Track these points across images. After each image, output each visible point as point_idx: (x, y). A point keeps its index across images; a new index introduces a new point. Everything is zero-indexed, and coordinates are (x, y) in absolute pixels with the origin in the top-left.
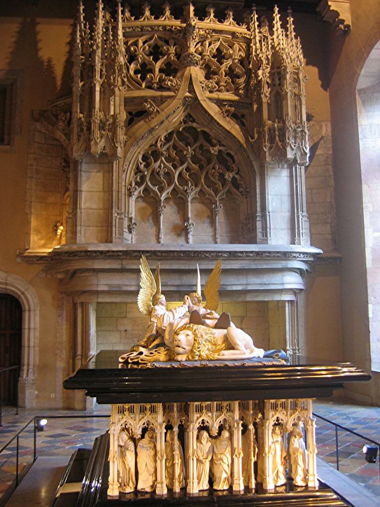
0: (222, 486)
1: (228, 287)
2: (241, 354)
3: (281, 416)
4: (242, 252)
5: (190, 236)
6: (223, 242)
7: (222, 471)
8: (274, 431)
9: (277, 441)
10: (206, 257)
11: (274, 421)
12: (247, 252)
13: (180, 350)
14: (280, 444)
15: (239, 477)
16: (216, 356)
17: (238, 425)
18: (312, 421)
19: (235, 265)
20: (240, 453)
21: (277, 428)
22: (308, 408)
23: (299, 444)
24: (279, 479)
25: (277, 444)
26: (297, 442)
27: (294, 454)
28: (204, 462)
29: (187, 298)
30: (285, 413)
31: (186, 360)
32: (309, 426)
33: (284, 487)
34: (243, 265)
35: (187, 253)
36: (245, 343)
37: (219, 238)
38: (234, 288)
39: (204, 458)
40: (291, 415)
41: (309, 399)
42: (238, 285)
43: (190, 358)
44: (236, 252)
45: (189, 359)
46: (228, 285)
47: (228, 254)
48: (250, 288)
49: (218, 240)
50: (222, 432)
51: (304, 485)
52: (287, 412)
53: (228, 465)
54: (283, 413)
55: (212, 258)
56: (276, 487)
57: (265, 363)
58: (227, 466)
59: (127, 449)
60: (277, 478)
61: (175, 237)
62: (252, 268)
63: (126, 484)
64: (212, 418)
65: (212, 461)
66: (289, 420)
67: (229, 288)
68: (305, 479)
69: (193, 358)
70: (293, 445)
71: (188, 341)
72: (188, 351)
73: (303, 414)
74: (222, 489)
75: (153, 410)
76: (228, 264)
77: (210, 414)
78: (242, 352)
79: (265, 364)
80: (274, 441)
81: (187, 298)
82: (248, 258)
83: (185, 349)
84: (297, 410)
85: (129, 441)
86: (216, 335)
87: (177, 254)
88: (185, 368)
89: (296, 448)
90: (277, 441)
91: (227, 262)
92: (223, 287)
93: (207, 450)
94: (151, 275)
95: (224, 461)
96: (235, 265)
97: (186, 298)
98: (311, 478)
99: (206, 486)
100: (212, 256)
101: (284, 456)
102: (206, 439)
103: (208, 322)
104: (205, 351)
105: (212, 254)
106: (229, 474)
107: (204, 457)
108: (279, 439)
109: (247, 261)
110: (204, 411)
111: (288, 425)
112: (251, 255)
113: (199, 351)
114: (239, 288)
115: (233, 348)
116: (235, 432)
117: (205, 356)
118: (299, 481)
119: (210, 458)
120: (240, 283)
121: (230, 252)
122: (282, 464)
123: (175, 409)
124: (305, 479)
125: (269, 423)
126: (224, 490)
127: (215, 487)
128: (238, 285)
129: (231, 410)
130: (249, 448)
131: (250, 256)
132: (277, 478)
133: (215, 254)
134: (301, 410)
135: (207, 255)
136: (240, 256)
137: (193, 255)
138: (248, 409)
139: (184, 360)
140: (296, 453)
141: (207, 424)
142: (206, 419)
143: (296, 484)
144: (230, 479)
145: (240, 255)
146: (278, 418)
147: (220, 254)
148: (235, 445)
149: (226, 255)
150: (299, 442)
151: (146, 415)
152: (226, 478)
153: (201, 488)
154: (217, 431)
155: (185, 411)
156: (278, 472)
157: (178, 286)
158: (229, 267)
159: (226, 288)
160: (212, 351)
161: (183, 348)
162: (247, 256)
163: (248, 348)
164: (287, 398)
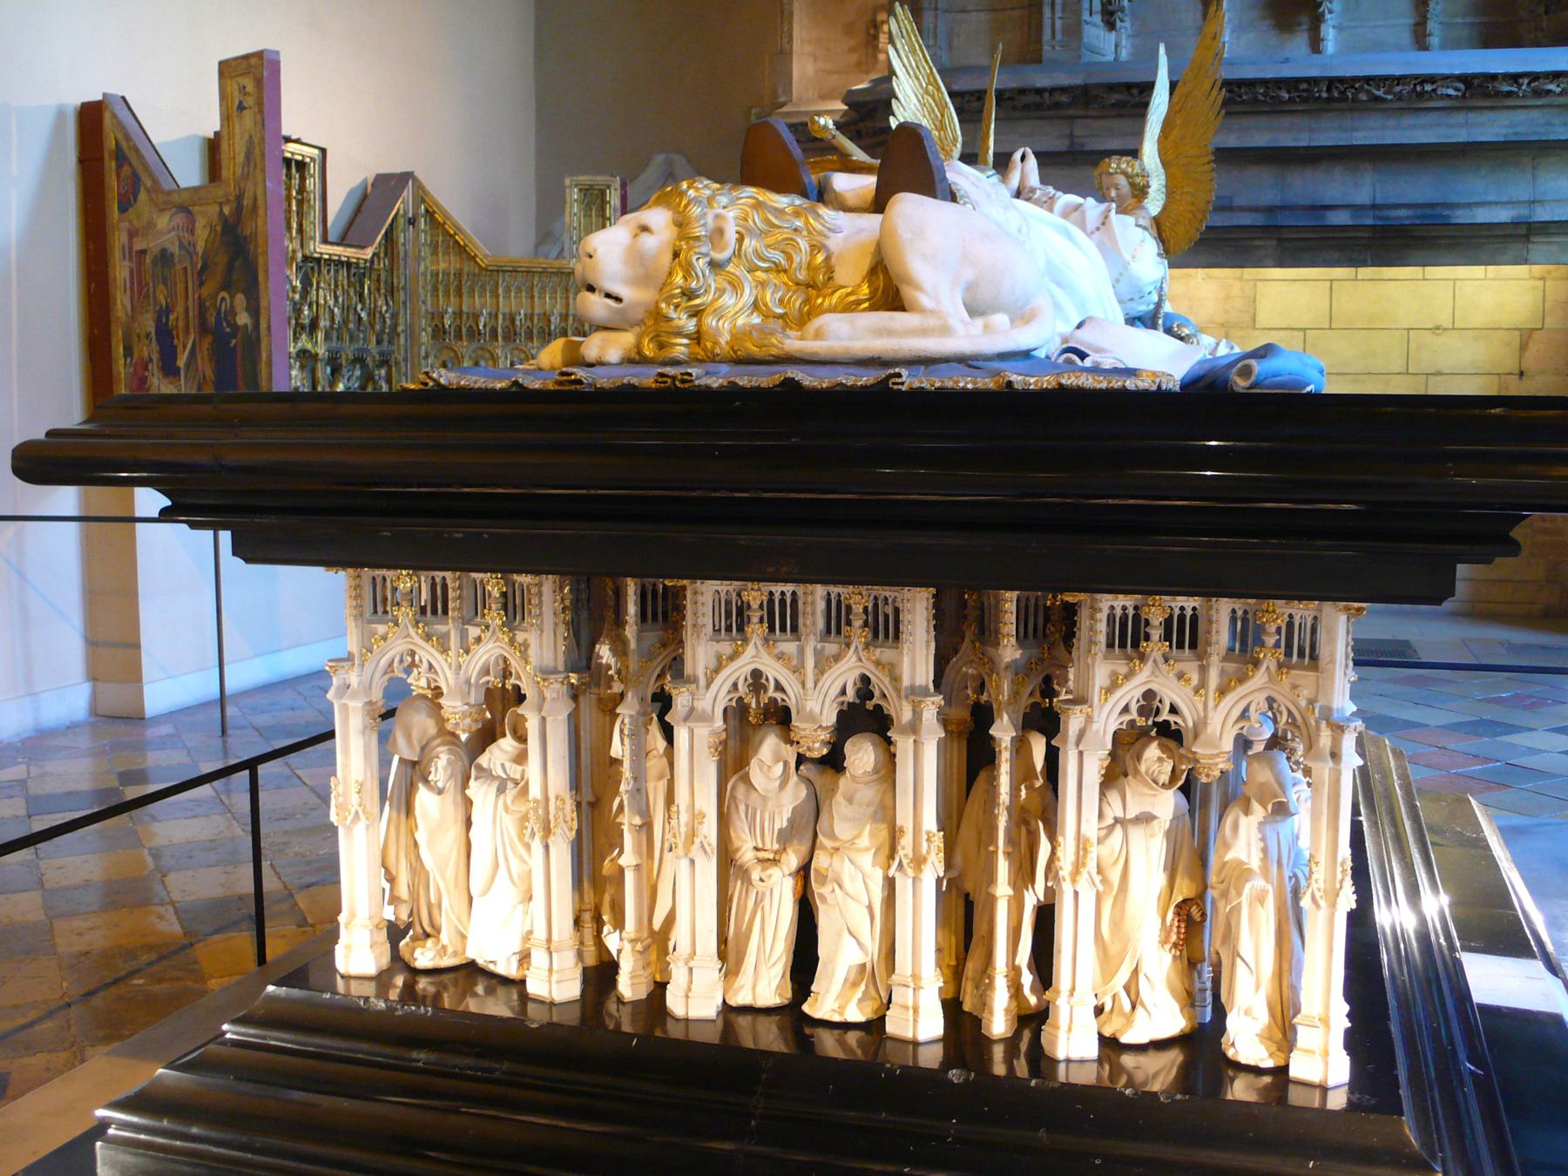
0: (834, 1001)
1: (1459, 212)
2: (923, 332)
3: (1171, 691)
4: (1515, 78)
5: (1329, 33)
6: (1450, 44)
7: (839, 935)
8: (1115, 774)
9: (1146, 819)
10: (1377, 99)
11: (1126, 710)
12: (1534, 77)
13: (595, 306)
14: (1168, 834)
15: (916, 977)
16: (793, 343)
17: (917, 714)
18: (1338, 729)
19: (1490, 126)
20: (925, 860)
21: (1153, 751)
22: (1323, 651)
23: (1265, 850)
24: (1139, 1009)
25: (1136, 833)
26: (1255, 835)
27: (1225, 895)
28: (755, 876)
29: (1023, 158)
30: (1195, 679)
31: (628, 361)
32: (1319, 757)
33: (1175, 1057)
34: (1520, 129)
35: (1304, 86)
36: (968, 275)
37: (1436, 32)
38: (1483, 216)
39: (760, 861)
40: (1222, 692)
41: (1328, 607)
42: (1497, 203)
43: (649, 350)
44: (1493, 77)
45: (639, 352)
46: (1469, 205)
47: (1462, 86)
48: (1543, 214)
49: (1434, 41)
50: (849, 747)
51: (1268, 1063)
52: (1203, 670)
53: (870, 908)
54: (1180, 676)
55: (1397, 105)
56: (1109, 1044)
57: (1014, 378)
58: (866, 913)
59: (426, 781)
60: (1134, 1007)
61: (1273, 38)
62: (1552, 137)
63: (429, 929)
64: (798, 670)
65: (804, 872)
66: (1219, 718)
67: (1462, 217)
68: (1284, 1031)
69: (661, 346)
70: (1227, 847)
71: (635, 256)
72: (639, 314)
73: (1294, 687)
74: (836, 1018)
75: (513, 608)
76: (1461, 126)
77: (789, 647)
78: (932, 322)
79: (1010, 383)
80: (1131, 814)
81: (1023, 158)
82: (1540, 102)
83: (618, 299)
84: (1256, 663)
85: (438, 741)
86: (834, 243)
87: (1265, 95)
88: (576, 392)
89: (1240, 863)
90: (1146, 819)
91: (1459, 118)
92: (1438, 211)
93: (782, 822)
94: (938, 89)
95: (847, 884)
96: (1490, 126)
97: (1018, 155)
98: (1305, 1037)
99: (764, 983)
100: (1399, 97)
101: (1178, 898)
102: (779, 768)
103: (842, 182)
104: (733, 313)
105: (1398, 89)
106: (873, 946)
107: (761, 855)
108: (1166, 804)
109: (1535, 114)
110: (756, 630)
111: (1202, 738)
112: (1552, 87)
113: (696, 313)
114: (1503, 215)
115: (902, 308)
116: (903, 745)
117: (724, 339)
118: (1246, 1040)
119: (792, 861)
120: (1505, 199)
121: (1466, 79)
122: (1163, 942)
123: (632, 609)
124: (1284, 1031)
125: (1089, 719)
126: (846, 1026)
127: (806, 1008)
128: (1497, 203)
129: (886, 629)
130: (993, 839)
131: (1549, 91)
132: (1134, 1007)
133: (1408, 88)
134: (1280, 666)
135: (1380, 93)
136: (1509, 94)
137: (1325, 95)
138: (987, 633)
139: (613, 355)
140: (1233, 891)
141: (778, 696)
142: (773, 670)
143: (1230, 1053)
144: (880, 973)
145: (1506, 88)
146: (1149, 695)
147: (1428, 88)
148: (904, 818)
149: (1451, 92)
150: (1263, 839)
151: (487, 627)
152: (863, 966)
153: (741, 998)
154: (825, 736)
155: (1053, 634)
156: (1136, 971)
157: (1270, 210)
158: (1462, 136)
159: (1448, 217)
160: (781, 316)
161: (608, 296)
162: (1538, 93)
163: (996, 308)
164: (1211, 589)
